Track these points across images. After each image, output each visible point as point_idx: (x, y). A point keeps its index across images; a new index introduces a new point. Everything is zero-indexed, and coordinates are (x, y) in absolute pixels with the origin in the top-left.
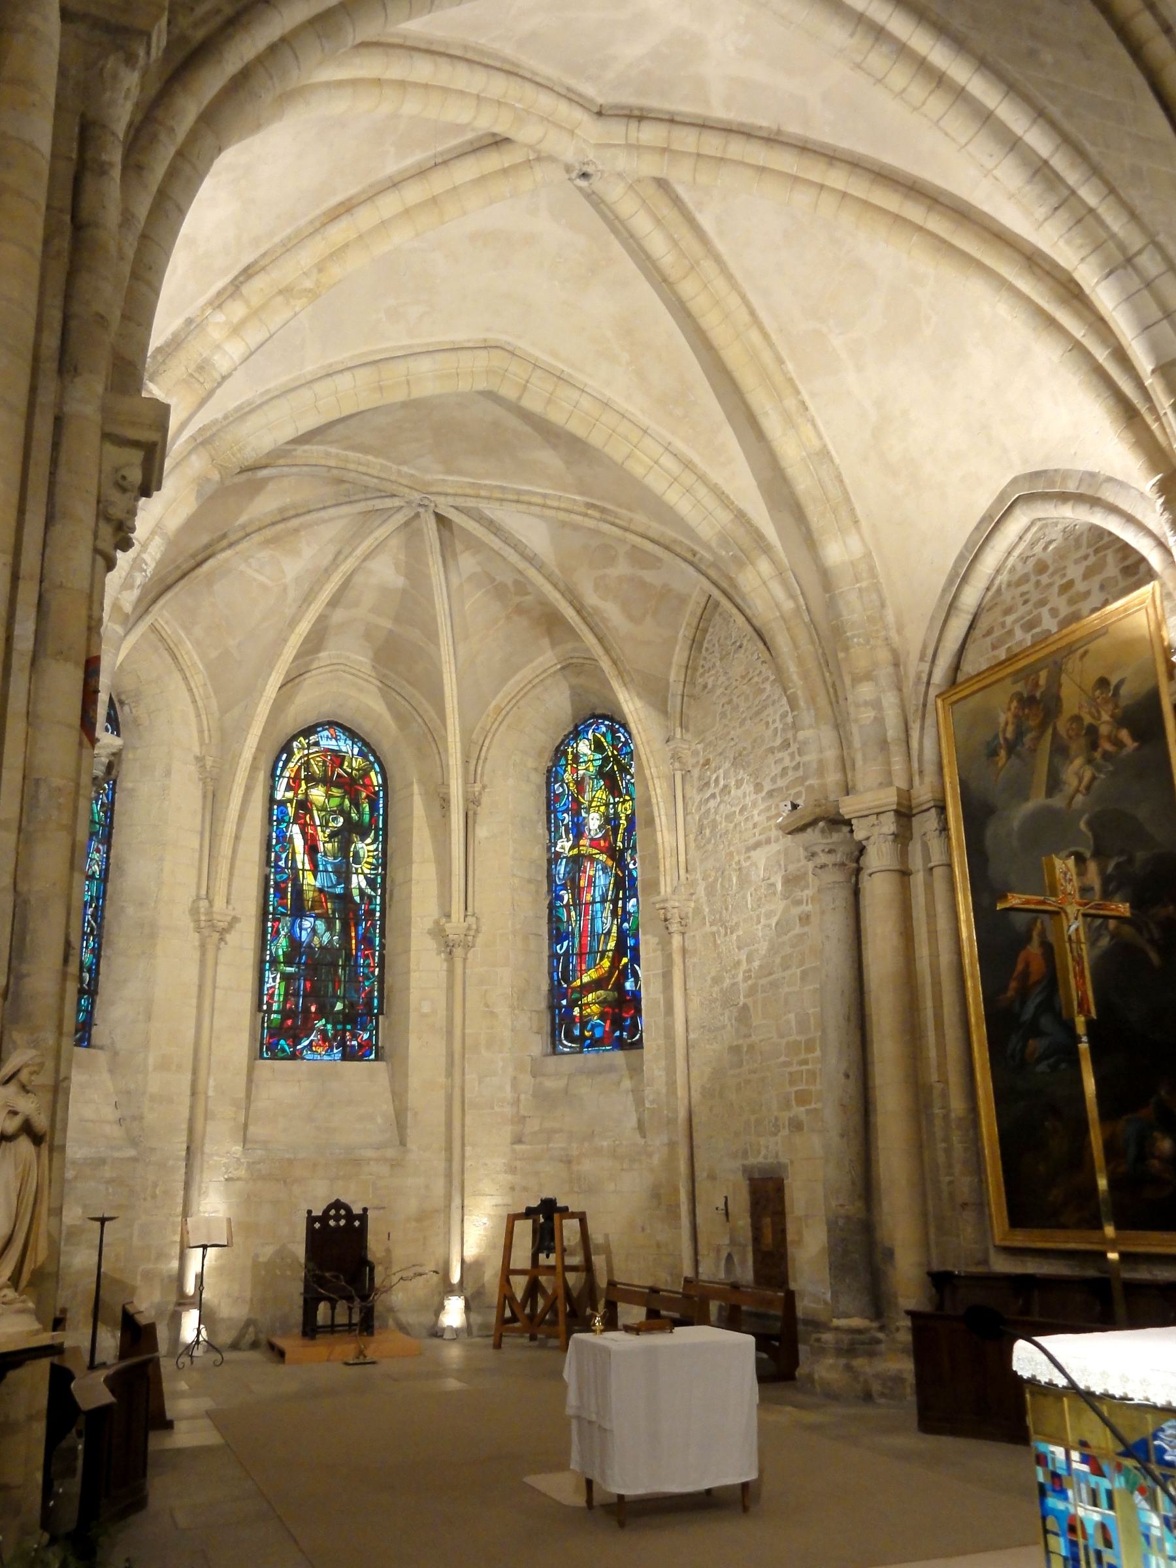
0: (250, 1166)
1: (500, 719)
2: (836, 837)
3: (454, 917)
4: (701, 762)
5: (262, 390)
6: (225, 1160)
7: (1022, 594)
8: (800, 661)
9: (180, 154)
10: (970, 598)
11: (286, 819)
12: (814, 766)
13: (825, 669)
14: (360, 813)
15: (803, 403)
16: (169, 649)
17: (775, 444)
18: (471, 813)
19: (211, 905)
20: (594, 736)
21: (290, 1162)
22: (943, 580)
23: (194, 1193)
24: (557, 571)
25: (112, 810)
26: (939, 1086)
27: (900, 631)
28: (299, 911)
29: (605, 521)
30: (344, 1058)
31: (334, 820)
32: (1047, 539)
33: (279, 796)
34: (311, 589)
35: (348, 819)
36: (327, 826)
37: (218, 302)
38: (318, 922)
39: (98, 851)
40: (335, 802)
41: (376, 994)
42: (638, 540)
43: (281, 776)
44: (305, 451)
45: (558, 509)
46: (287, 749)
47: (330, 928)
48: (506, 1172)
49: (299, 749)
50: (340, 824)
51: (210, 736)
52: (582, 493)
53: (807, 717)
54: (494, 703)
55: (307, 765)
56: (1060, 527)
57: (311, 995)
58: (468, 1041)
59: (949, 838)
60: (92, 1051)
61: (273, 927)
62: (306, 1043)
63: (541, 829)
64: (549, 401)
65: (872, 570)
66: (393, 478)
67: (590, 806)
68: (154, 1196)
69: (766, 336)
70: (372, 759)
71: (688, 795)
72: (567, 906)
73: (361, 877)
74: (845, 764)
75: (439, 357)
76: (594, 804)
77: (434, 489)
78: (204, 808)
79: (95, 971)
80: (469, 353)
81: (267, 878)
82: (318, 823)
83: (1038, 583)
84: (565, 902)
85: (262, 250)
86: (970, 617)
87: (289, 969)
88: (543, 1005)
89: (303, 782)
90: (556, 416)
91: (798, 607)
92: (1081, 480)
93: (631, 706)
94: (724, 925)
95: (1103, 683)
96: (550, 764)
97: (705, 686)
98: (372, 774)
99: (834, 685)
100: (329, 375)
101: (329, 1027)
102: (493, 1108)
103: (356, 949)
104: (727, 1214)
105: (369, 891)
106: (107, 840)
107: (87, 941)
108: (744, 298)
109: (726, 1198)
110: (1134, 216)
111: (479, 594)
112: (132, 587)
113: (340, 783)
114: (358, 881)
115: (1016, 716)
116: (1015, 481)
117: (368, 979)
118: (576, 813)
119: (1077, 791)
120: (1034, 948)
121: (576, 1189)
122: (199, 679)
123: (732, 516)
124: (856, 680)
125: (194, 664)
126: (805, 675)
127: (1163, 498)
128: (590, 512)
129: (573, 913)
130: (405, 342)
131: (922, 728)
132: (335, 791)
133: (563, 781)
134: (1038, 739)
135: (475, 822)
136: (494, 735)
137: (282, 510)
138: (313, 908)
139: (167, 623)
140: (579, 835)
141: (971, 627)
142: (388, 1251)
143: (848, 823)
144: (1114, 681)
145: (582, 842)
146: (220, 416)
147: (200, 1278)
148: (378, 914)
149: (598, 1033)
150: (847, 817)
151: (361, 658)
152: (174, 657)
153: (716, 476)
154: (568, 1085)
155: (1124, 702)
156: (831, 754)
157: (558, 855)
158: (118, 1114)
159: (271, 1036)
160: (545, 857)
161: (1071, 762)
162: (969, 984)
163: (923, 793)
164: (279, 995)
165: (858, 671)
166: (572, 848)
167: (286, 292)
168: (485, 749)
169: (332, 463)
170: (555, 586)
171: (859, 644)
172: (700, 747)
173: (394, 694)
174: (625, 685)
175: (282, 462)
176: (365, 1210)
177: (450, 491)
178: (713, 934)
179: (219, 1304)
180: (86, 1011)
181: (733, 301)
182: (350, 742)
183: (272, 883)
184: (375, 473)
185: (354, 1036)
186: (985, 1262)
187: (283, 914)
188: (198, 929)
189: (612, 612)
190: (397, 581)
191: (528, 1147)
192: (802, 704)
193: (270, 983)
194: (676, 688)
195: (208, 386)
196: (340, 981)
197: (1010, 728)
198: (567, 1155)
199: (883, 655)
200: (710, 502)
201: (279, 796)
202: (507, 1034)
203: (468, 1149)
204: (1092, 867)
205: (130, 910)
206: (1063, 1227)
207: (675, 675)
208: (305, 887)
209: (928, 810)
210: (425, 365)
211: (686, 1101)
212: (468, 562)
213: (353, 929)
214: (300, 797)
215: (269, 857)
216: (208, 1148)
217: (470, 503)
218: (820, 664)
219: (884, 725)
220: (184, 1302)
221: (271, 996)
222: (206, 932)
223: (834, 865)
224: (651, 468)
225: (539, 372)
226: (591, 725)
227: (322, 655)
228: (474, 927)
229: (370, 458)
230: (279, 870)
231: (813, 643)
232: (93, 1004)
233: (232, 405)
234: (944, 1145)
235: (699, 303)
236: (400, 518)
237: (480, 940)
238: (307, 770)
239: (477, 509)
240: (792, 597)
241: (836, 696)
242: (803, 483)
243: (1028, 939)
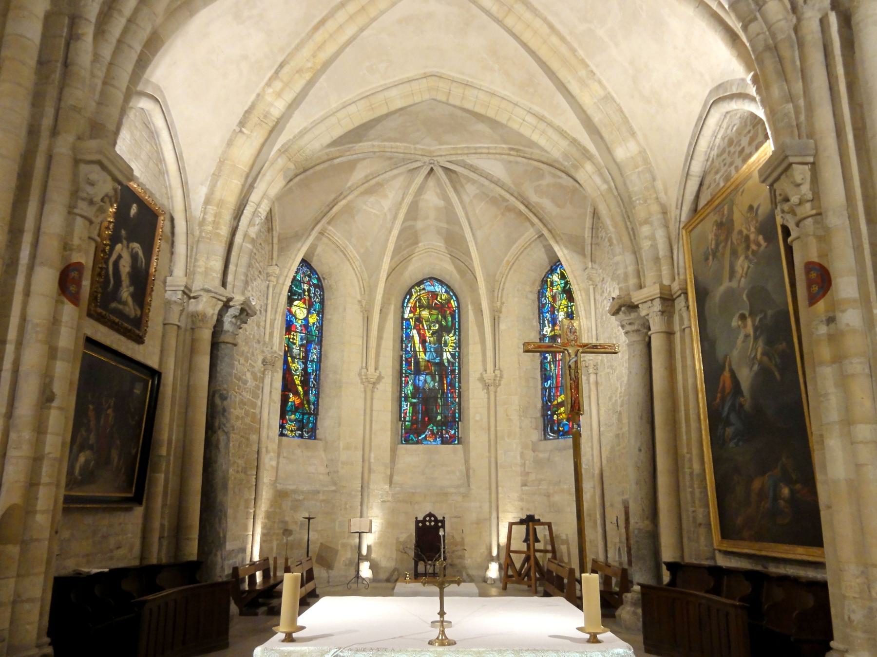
0: (393, 495)
1: (509, 267)
2: (633, 315)
3: (488, 372)
4: (601, 279)
5: (311, 120)
6: (380, 492)
7: (724, 160)
8: (612, 218)
9: (130, 21)
10: (697, 168)
11: (410, 327)
12: (622, 276)
13: (627, 220)
14: (447, 321)
15: (592, 72)
16: (342, 251)
17: (577, 98)
18: (496, 318)
19: (367, 370)
20: (561, 271)
21: (413, 493)
22: (683, 159)
23: (365, 508)
24: (512, 186)
25: (322, 330)
26: (688, 456)
27: (666, 193)
28: (418, 372)
29: (520, 156)
30: (443, 443)
31: (433, 326)
32: (733, 124)
33: (406, 316)
34: (396, 214)
35: (441, 325)
36: (430, 329)
37: (269, 84)
38: (427, 377)
39: (315, 349)
40: (435, 317)
41: (457, 411)
42: (536, 163)
43: (407, 306)
44: (360, 146)
45: (496, 154)
46: (409, 293)
47: (433, 379)
48: (519, 501)
49: (415, 292)
50: (437, 328)
51: (364, 290)
52: (505, 142)
53: (618, 249)
54: (505, 261)
55: (420, 300)
56: (738, 115)
58: (499, 434)
59: (689, 311)
60: (316, 441)
61: (405, 380)
62: (423, 436)
63: (535, 323)
64: (463, 98)
65: (646, 160)
66: (412, 152)
67: (559, 309)
68: (346, 509)
69: (562, 39)
70: (451, 294)
71: (597, 298)
72: (549, 362)
73: (448, 353)
74: (638, 274)
75: (400, 86)
76: (561, 307)
77: (435, 154)
78: (363, 325)
79: (317, 404)
80: (417, 81)
81: (402, 357)
82: (426, 328)
83: (729, 152)
84: (548, 360)
85: (286, 54)
86: (699, 179)
88: (539, 414)
89: (418, 309)
90: (469, 106)
91: (610, 188)
92: (738, 84)
93: (562, 253)
94: (612, 369)
95: (751, 208)
96: (539, 288)
97: (602, 238)
98: (452, 301)
99: (633, 229)
100: (344, 107)
101: (434, 428)
102: (511, 467)
103: (447, 390)
104: (618, 526)
105: (452, 360)
106: (320, 343)
107: (312, 391)
108: (545, 20)
109: (617, 517)
111: (483, 204)
112: (254, 225)
113: (436, 307)
114: (446, 356)
115: (716, 235)
116: (711, 92)
117: (453, 404)
118: (553, 313)
119: (742, 276)
120: (727, 374)
121: (552, 510)
122: (357, 263)
123: (567, 142)
124: (641, 225)
125: (355, 257)
126: (615, 225)
127: (755, 87)
128: (512, 153)
129: (552, 366)
130: (382, 82)
131: (678, 248)
132: (434, 312)
133: (546, 296)
134: (725, 247)
135: (499, 322)
136: (507, 276)
137: (366, 177)
138: (424, 370)
139: (339, 239)
141: (701, 185)
142: (463, 539)
143: (637, 307)
144: (755, 206)
145: (556, 328)
146: (291, 137)
147: (369, 547)
148: (457, 371)
149: (566, 429)
150: (636, 303)
151: (439, 244)
152: (345, 255)
153: (557, 122)
154: (549, 456)
155: (760, 219)
156: (631, 269)
157: (544, 336)
158: (328, 470)
159: (406, 433)
160: (538, 337)
161: (739, 259)
162: (700, 396)
163: (676, 287)
164: (409, 413)
165: (640, 219)
166: (551, 332)
167: (300, 71)
168: (502, 283)
169: (376, 150)
170: (512, 195)
171: (640, 204)
172: (601, 271)
173: (457, 261)
174: (557, 242)
175: (348, 153)
176: (444, 518)
177: (443, 154)
178: (609, 373)
179: (381, 561)
180: (313, 423)
181: (538, 23)
182: (440, 287)
183: (404, 359)
184: (402, 151)
185: (447, 433)
186: (713, 558)
187: (410, 374)
188: (362, 383)
189: (547, 205)
190: (442, 203)
191: (529, 488)
192: (615, 241)
193: (404, 407)
194: (588, 241)
195: (271, 124)
196: (439, 405)
197: (713, 242)
198: (548, 493)
199: (655, 208)
200: (555, 137)
201: (406, 316)
202: (518, 430)
203: (500, 488)
204: (749, 322)
205: (331, 376)
206: (742, 539)
207: (587, 234)
208: (420, 360)
209: (680, 296)
210: (393, 93)
211: (599, 465)
212: (471, 190)
213: (445, 379)
214: (416, 316)
215: (402, 346)
216: (371, 486)
217: (454, 158)
218: (624, 218)
219: (657, 248)
220: (361, 558)
221: (406, 414)
222: (366, 384)
223: (633, 331)
224: (522, 124)
225: (454, 84)
226: (559, 265)
227: (420, 245)
228: (499, 376)
229: (398, 144)
230: (407, 352)
231: (619, 206)
232: (316, 419)
233: (297, 131)
234: (690, 490)
235: (518, 28)
236: (425, 171)
237: (502, 383)
238: (419, 302)
239: (463, 160)
240: (605, 181)
241: (633, 235)
242: (597, 118)
243: (723, 368)
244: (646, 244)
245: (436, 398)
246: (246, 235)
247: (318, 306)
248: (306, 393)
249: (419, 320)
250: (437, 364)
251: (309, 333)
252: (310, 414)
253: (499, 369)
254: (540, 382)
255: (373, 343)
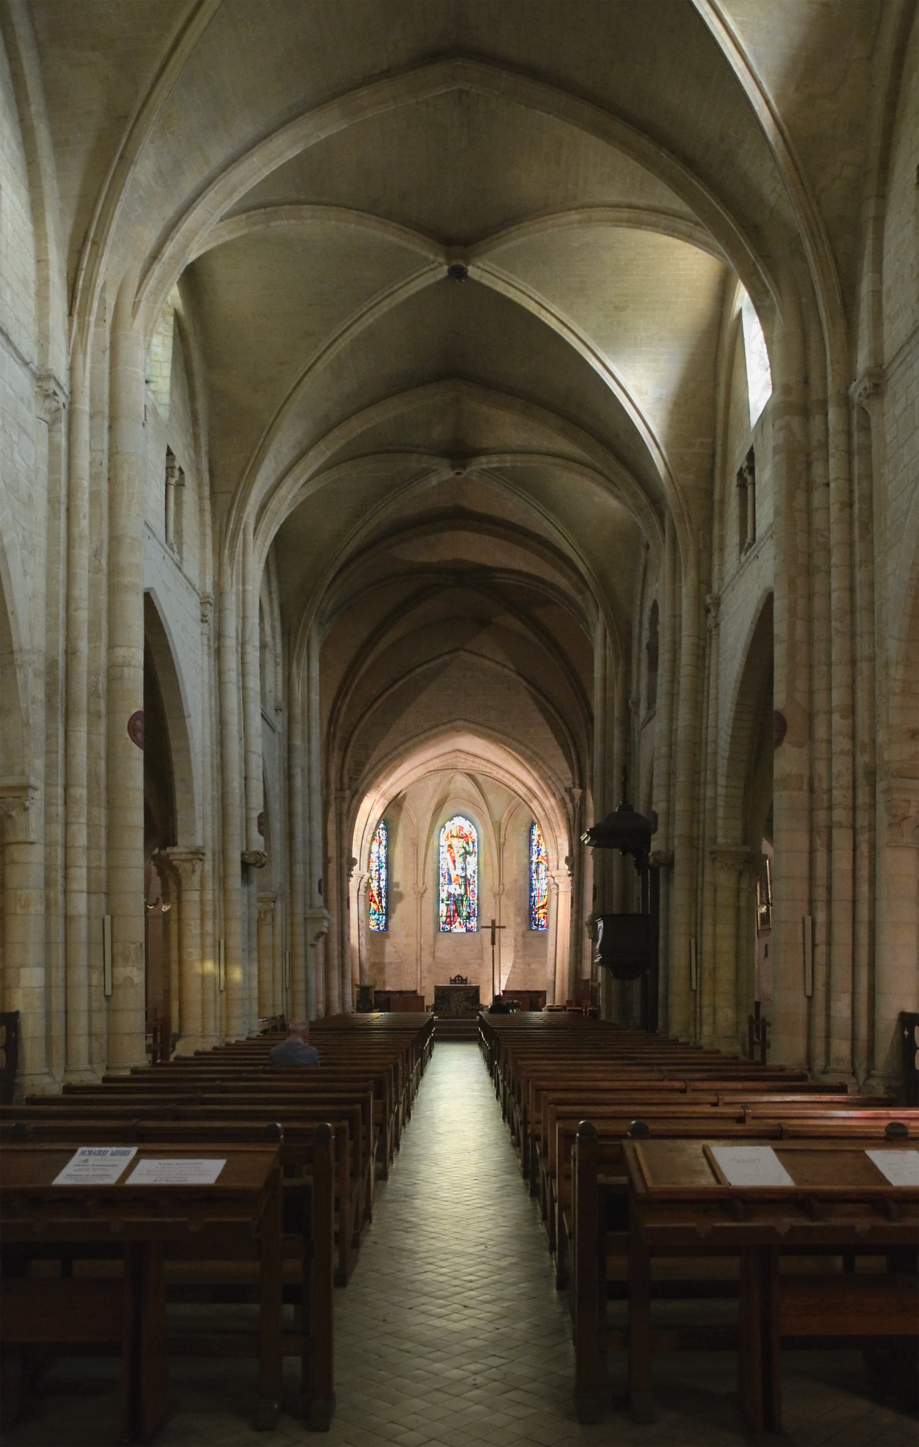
28: (450, 882)
57: (456, 911)
70: (472, 826)
87: (449, 902)
110: (550, 768)
114: (469, 872)
132: (462, 840)
140: (539, 855)
188: (415, 894)
200: (521, 786)
244: (559, 847)
245: (462, 901)
246: (367, 840)
247: (384, 843)
248: (380, 902)
249: (450, 846)
250: (461, 877)
251: (380, 862)
252: (383, 914)
253: (503, 885)
254: (528, 893)
255: (421, 867)
